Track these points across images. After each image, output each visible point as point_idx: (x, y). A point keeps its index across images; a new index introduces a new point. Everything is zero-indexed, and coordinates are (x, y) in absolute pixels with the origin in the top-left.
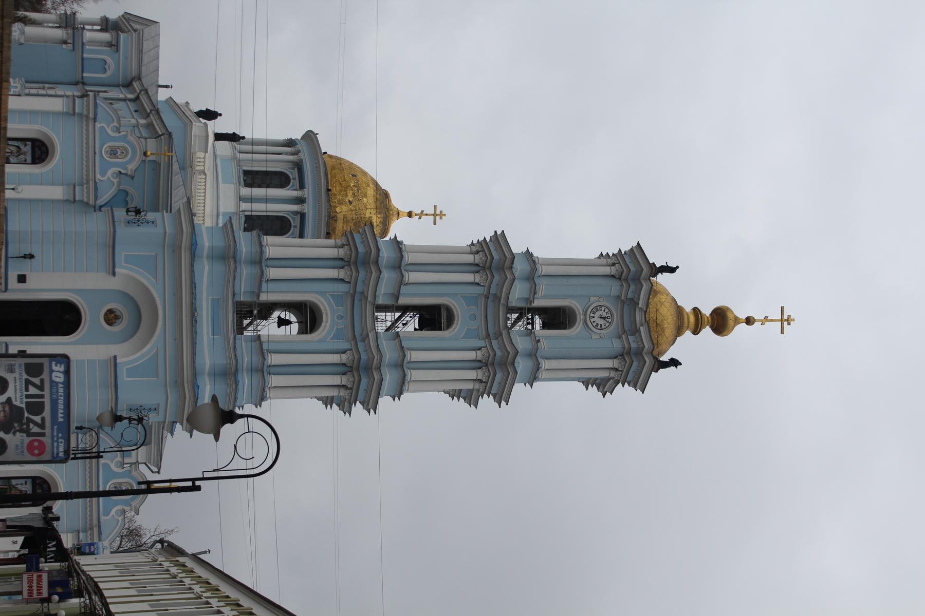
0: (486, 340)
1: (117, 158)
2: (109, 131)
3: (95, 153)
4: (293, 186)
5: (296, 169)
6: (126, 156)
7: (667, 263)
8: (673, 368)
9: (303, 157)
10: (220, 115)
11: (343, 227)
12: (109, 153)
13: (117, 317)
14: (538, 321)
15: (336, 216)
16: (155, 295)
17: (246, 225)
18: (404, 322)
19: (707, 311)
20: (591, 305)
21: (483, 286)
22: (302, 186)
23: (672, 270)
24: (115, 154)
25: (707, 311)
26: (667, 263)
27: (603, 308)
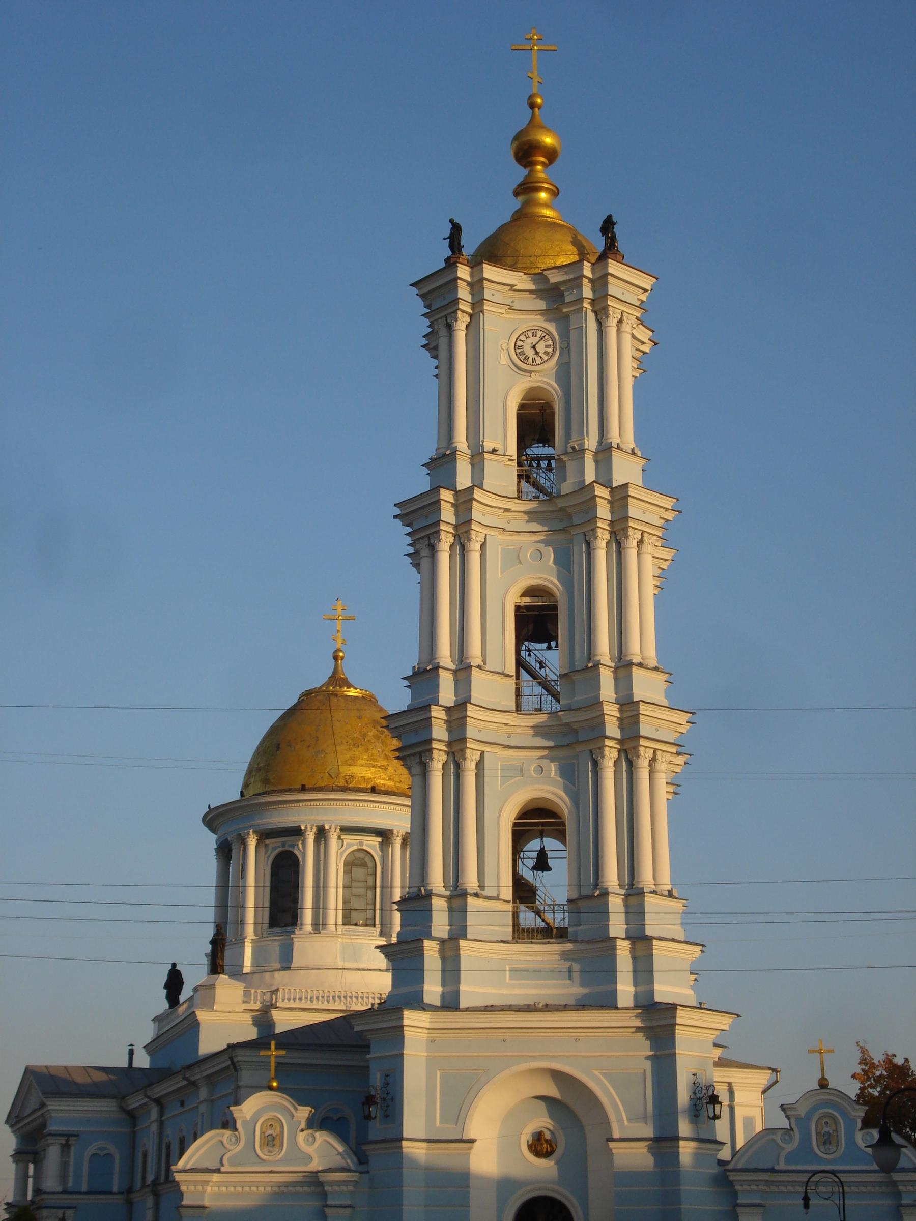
0: (573, 533)
3: (271, 1172)
7: (445, 239)
8: (616, 229)
12: (271, 1149)
14: (537, 450)
18: (538, 665)
21: (485, 539)
23: (456, 229)
24: (274, 1139)
25: (519, 173)
26: (445, 239)
27: (519, 343)
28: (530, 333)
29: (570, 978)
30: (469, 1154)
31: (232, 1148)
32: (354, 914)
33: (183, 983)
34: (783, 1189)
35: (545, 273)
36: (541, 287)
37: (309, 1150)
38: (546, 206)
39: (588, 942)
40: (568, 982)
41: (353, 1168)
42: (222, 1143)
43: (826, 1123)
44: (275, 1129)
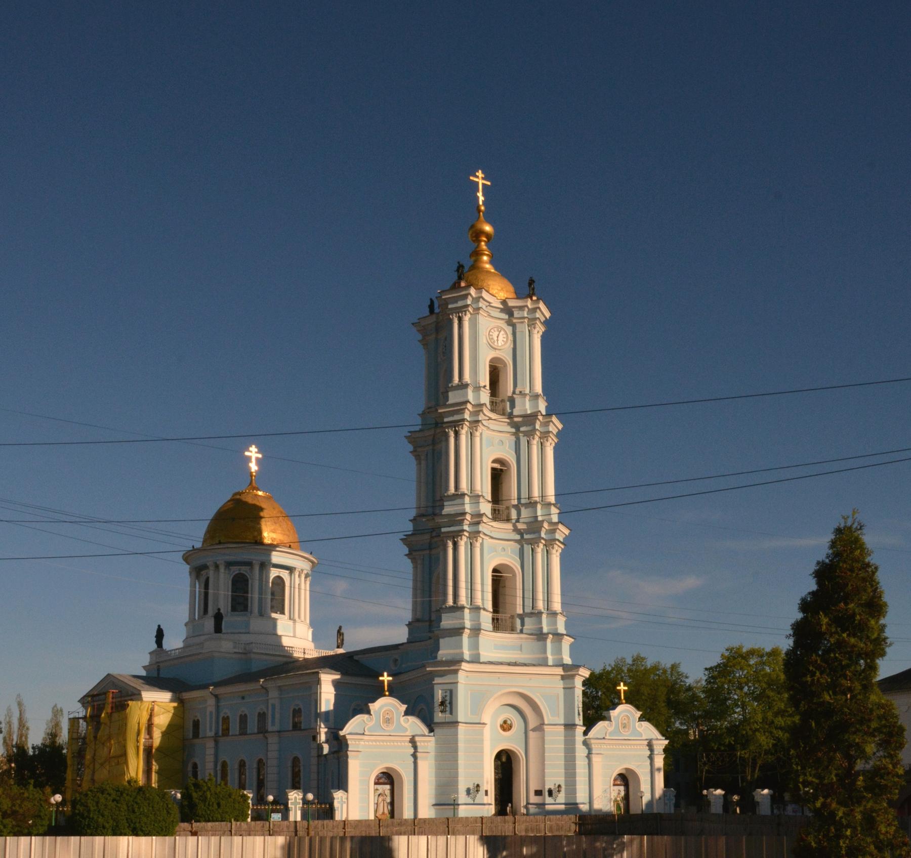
4: (246, 572)
5: (230, 567)
11: (279, 533)
12: (388, 724)
13: (505, 722)
15: (271, 538)
16: (499, 693)
22: (249, 564)
27: (491, 333)
29: (521, 650)
30: (483, 730)
31: (369, 723)
33: (163, 635)
35: (507, 300)
38: (486, 263)
40: (520, 652)
41: (427, 734)
43: (625, 719)
44: (390, 715)
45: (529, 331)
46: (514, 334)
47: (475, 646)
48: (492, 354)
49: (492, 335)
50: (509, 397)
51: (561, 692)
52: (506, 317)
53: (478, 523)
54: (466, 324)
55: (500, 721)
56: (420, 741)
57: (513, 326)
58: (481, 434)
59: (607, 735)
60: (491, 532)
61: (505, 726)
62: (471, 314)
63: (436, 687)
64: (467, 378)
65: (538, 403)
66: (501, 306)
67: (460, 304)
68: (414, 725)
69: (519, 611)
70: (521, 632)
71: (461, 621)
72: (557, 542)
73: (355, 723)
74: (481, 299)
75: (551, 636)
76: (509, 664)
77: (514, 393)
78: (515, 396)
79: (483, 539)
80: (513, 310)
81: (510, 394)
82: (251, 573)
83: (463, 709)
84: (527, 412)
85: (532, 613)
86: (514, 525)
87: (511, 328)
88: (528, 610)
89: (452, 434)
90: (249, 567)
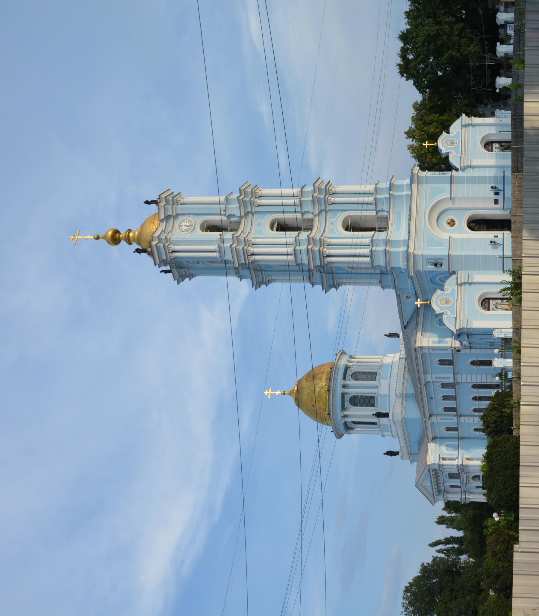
1: (445, 299)
2: (449, 313)
4: (348, 397)
5: (345, 407)
6: (440, 300)
8: (149, 200)
9: (341, 412)
10: (384, 454)
13: (449, 223)
16: (429, 227)
17: (376, 376)
19: (123, 243)
20: (191, 232)
22: (343, 395)
27: (184, 231)
28: (180, 227)
32: (373, 378)
34: (466, 154)
36: (165, 220)
37: (450, 290)
39: (390, 206)
41: (456, 276)
42: (447, 318)
45: (181, 204)
46: (183, 214)
47: (397, 243)
48: (198, 230)
49: (185, 230)
50: (227, 218)
51: (429, 186)
52: (172, 219)
53: (314, 241)
54: (177, 248)
55: (448, 227)
56: (461, 280)
57: (177, 215)
58: (253, 238)
59: (458, 155)
60: (321, 232)
61: (451, 224)
62: (170, 244)
63: (425, 270)
64: (214, 247)
65: (232, 199)
66: (165, 223)
67: (163, 251)
68: (450, 284)
69: (374, 213)
70: (389, 212)
71: (381, 251)
72: (328, 187)
73: (449, 324)
74: (160, 237)
75: (391, 192)
76: (410, 220)
77: (225, 215)
78: (227, 215)
79: (325, 237)
80: (166, 215)
81: (224, 218)
82: (349, 393)
83: (441, 252)
84: (237, 207)
85: (376, 205)
86: (315, 216)
87: (179, 217)
88: (373, 207)
89: (253, 257)
90: (345, 395)
